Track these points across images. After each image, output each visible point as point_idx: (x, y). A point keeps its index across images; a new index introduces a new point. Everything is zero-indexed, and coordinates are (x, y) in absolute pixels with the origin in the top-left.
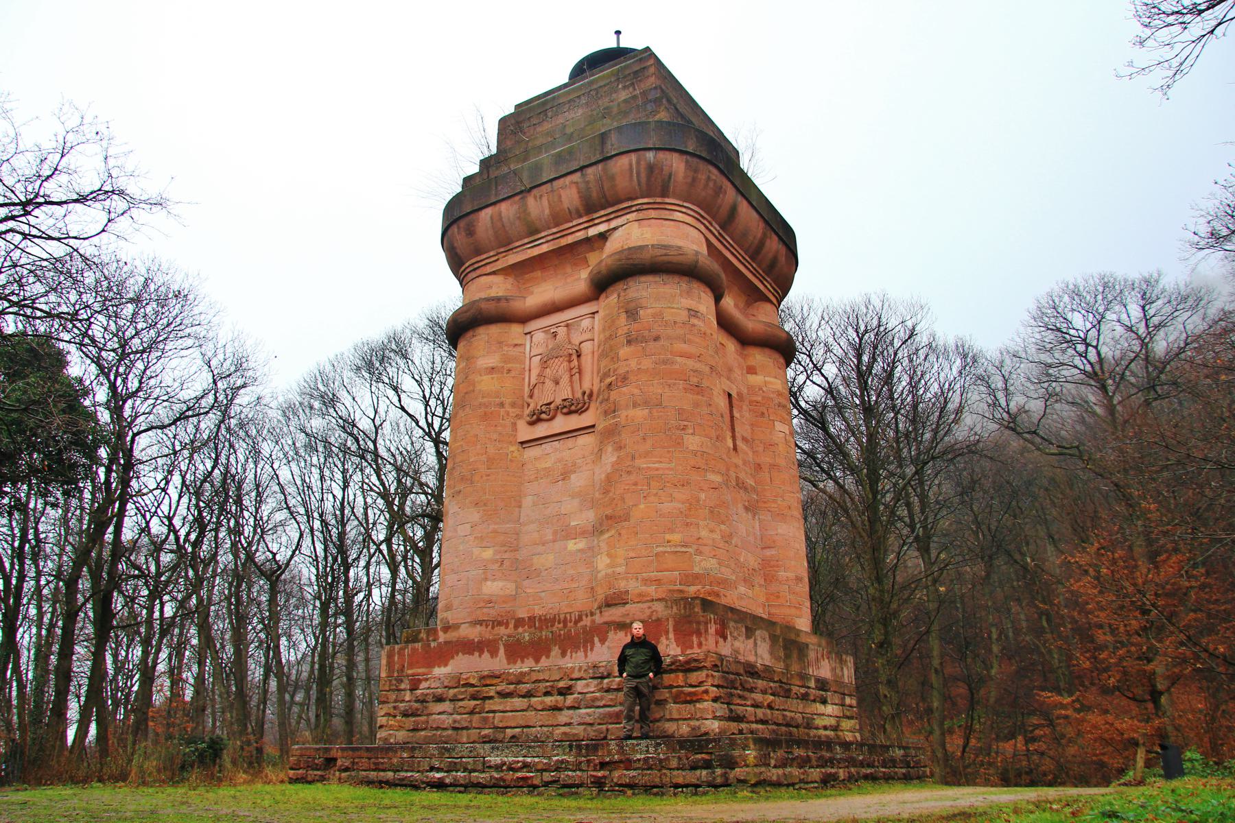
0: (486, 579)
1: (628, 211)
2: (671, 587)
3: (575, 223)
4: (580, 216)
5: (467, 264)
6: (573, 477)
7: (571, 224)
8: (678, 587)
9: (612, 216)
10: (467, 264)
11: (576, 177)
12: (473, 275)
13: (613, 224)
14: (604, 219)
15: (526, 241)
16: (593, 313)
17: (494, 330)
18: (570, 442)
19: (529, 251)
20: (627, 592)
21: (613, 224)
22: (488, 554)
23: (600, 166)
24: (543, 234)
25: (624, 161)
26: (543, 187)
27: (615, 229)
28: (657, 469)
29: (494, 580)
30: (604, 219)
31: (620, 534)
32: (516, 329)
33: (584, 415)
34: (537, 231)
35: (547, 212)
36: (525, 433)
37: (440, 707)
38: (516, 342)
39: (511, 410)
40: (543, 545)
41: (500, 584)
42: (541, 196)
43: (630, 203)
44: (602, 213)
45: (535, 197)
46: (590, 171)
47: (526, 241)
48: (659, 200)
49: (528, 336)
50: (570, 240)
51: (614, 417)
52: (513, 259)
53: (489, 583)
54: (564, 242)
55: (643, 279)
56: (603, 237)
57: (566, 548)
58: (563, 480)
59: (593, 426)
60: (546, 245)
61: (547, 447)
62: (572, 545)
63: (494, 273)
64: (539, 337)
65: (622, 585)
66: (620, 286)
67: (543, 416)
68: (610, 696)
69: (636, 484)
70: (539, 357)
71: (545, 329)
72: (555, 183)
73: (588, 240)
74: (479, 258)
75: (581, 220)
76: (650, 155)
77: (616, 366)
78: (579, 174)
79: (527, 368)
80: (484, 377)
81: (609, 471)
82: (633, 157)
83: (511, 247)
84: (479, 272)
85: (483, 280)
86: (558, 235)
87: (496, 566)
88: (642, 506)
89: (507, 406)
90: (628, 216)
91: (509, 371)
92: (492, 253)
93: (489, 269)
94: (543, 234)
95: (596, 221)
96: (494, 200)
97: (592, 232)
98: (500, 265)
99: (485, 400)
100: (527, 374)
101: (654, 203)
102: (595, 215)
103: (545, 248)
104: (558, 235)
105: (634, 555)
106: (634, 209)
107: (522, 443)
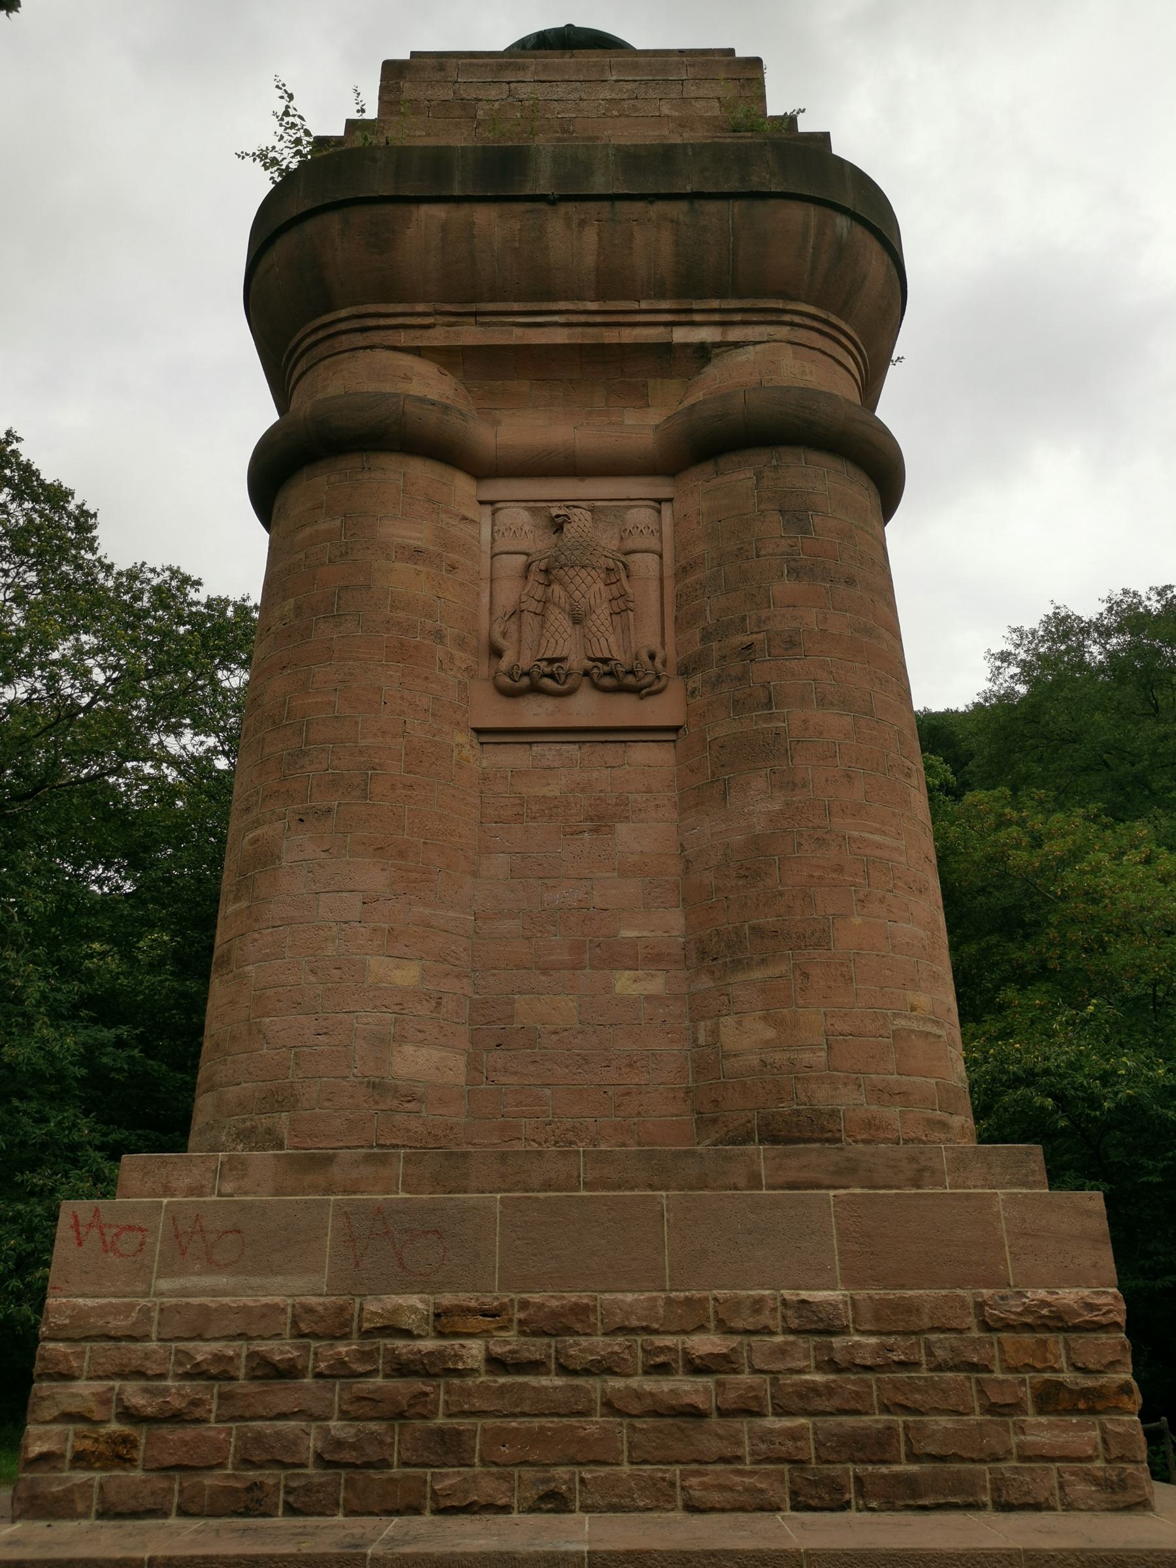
0: (402, 1039)
1: (772, 317)
2: (929, 1114)
3: (644, 305)
4: (662, 296)
5: (343, 313)
6: (621, 828)
7: (635, 306)
8: (938, 1115)
9: (738, 317)
10: (343, 313)
11: (678, 210)
12: (359, 340)
13: (735, 334)
14: (717, 317)
15: (516, 306)
16: (659, 501)
17: (421, 471)
18: (610, 753)
19: (518, 331)
20: (833, 1114)
21: (735, 334)
22: (407, 975)
23: (737, 207)
24: (562, 305)
25: (795, 213)
26: (591, 206)
27: (737, 345)
28: (880, 846)
29: (421, 1043)
30: (717, 317)
31: (806, 975)
32: (463, 486)
33: (651, 702)
34: (550, 296)
35: (590, 260)
36: (498, 713)
37: (283, 1396)
38: (465, 511)
39: (458, 654)
40: (545, 971)
41: (436, 1054)
42: (582, 223)
43: (780, 305)
44: (715, 304)
45: (568, 220)
46: (712, 207)
47: (516, 306)
48: (834, 319)
49: (488, 510)
50: (628, 336)
51: (770, 718)
52: (471, 335)
53: (409, 1049)
54: (612, 336)
55: (815, 457)
56: (703, 353)
57: (608, 988)
58: (596, 830)
59: (675, 729)
60: (566, 331)
61: (549, 753)
62: (625, 983)
63: (417, 351)
64: (517, 516)
65: (822, 1096)
66: (761, 458)
67: (548, 683)
68: (850, 1382)
69: (839, 869)
70: (524, 558)
71: (533, 506)
72: (623, 207)
73: (667, 348)
74: (382, 308)
75: (665, 305)
76: (842, 223)
77: (764, 613)
78: (683, 206)
79: (486, 573)
80: (398, 565)
81: (758, 829)
82: (813, 211)
83: (473, 308)
84: (375, 337)
85: (384, 356)
86: (598, 319)
87: (424, 1009)
88: (857, 920)
89: (448, 640)
90: (770, 329)
91: (453, 568)
92: (420, 308)
93: (404, 338)
94: (562, 305)
95: (698, 318)
96: (457, 192)
97: (680, 335)
98: (438, 337)
99: (401, 614)
100: (486, 587)
101: (826, 322)
102: (696, 305)
103: (560, 337)
104: (598, 319)
105: (846, 1028)
106: (787, 318)
107: (479, 731)
